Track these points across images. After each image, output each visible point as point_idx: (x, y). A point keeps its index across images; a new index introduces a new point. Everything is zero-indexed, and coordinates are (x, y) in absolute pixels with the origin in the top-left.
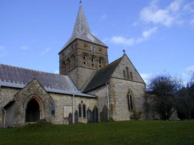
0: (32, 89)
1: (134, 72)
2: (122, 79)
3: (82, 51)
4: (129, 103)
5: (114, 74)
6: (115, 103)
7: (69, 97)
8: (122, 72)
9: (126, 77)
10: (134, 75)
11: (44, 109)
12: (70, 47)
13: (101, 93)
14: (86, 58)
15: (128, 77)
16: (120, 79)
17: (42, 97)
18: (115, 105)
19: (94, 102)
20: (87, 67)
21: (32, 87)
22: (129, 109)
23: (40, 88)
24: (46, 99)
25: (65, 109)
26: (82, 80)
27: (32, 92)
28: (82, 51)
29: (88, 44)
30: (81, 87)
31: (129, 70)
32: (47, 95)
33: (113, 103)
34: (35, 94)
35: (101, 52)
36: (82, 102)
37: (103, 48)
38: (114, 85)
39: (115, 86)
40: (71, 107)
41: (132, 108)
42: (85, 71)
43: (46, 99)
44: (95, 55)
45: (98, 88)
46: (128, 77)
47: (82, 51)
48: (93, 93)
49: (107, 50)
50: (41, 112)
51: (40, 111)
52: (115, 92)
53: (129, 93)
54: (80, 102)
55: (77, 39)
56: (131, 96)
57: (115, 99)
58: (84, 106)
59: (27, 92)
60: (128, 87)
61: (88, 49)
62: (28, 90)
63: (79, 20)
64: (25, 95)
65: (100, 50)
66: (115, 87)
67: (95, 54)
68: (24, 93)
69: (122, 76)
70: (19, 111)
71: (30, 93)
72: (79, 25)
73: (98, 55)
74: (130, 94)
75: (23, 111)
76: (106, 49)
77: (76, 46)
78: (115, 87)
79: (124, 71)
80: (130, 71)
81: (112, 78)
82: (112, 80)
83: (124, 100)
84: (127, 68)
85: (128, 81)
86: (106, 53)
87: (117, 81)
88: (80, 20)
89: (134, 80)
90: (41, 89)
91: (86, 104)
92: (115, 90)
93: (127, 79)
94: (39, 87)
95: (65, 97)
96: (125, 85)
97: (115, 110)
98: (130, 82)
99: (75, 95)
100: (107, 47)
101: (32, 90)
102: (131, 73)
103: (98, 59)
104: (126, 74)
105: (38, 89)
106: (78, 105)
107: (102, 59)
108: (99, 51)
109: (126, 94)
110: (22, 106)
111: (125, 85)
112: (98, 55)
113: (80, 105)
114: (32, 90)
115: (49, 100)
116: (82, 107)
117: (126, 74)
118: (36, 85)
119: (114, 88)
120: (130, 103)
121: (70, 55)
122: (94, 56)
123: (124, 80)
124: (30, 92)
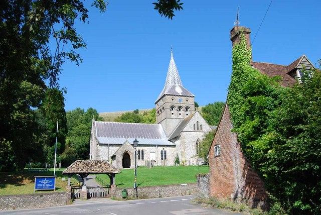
10: (203, 127)
15: (198, 129)
46: (198, 129)
58: (165, 152)
65: (187, 101)
69: (192, 129)
73: (184, 105)
80: (199, 124)
113: (162, 151)
116: (163, 153)
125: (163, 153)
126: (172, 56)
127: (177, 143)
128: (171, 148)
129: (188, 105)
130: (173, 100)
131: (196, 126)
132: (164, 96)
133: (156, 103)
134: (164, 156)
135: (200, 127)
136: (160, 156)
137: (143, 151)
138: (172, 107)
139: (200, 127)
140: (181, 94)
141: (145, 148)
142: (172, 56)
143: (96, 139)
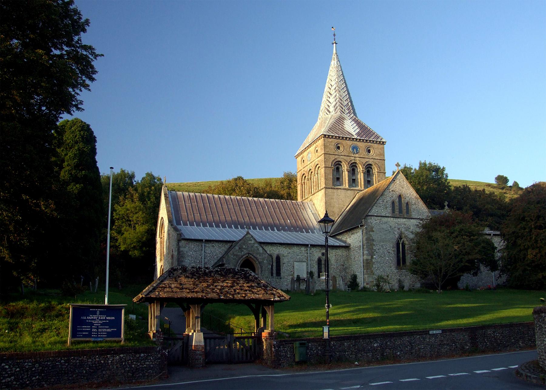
0: (244, 247)
2: (389, 217)
4: (398, 257)
5: (374, 211)
6: (372, 257)
7: (303, 249)
8: (389, 205)
9: (397, 211)
12: (312, 148)
13: (354, 239)
15: (401, 211)
16: (384, 217)
17: (258, 256)
19: (344, 254)
23: (255, 245)
24: (263, 259)
25: (296, 267)
27: (245, 251)
29: (344, 142)
34: (248, 254)
38: (372, 228)
39: (374, 229)
40: (305, 264)
43: (263, 259)
45: (351, 230)
47: (332, 158)
48: (344, 237)
49: (384, 148)
52: (373, 240)
53: (401, 238)
54: (320, 255)
58: (327, 260)
60: (399, 229)
63: (330, 87)
64: (237, 255)
66: (373, 231)
68: (235, 253)
69: (388, 211)
76: (381, 146)
78: (373, 231)
79: (393, 203)
81: (369, 217)
82: (369, 221)
83: (389, 252)
85: (399, 220)
86: (383, 154)
87: (378, 221)
89: (414, 216)
92: (374, 236)
95: (296, 249)
96: (393, 227)
97: (371, 269)
98: (404, 220)
99: (311, 245)
100: (383, 143)
102: (407, 204)
104: (397, 208)
105: (252, 247)
106: (316, 260)
109: (395, 241)
111: (393, 227)
113: (319, 261)
114: (245, 249)
117: (397, 208)
119: (371, 233)
120: (401, 256)
121: (313, 163)
123: (392, 219)
131: (397, 204)
136: (315, 270)
137: (278, 258)
139: (404, 207)
140: (356, 137)
141: (283, 251)
143: (176, 229)
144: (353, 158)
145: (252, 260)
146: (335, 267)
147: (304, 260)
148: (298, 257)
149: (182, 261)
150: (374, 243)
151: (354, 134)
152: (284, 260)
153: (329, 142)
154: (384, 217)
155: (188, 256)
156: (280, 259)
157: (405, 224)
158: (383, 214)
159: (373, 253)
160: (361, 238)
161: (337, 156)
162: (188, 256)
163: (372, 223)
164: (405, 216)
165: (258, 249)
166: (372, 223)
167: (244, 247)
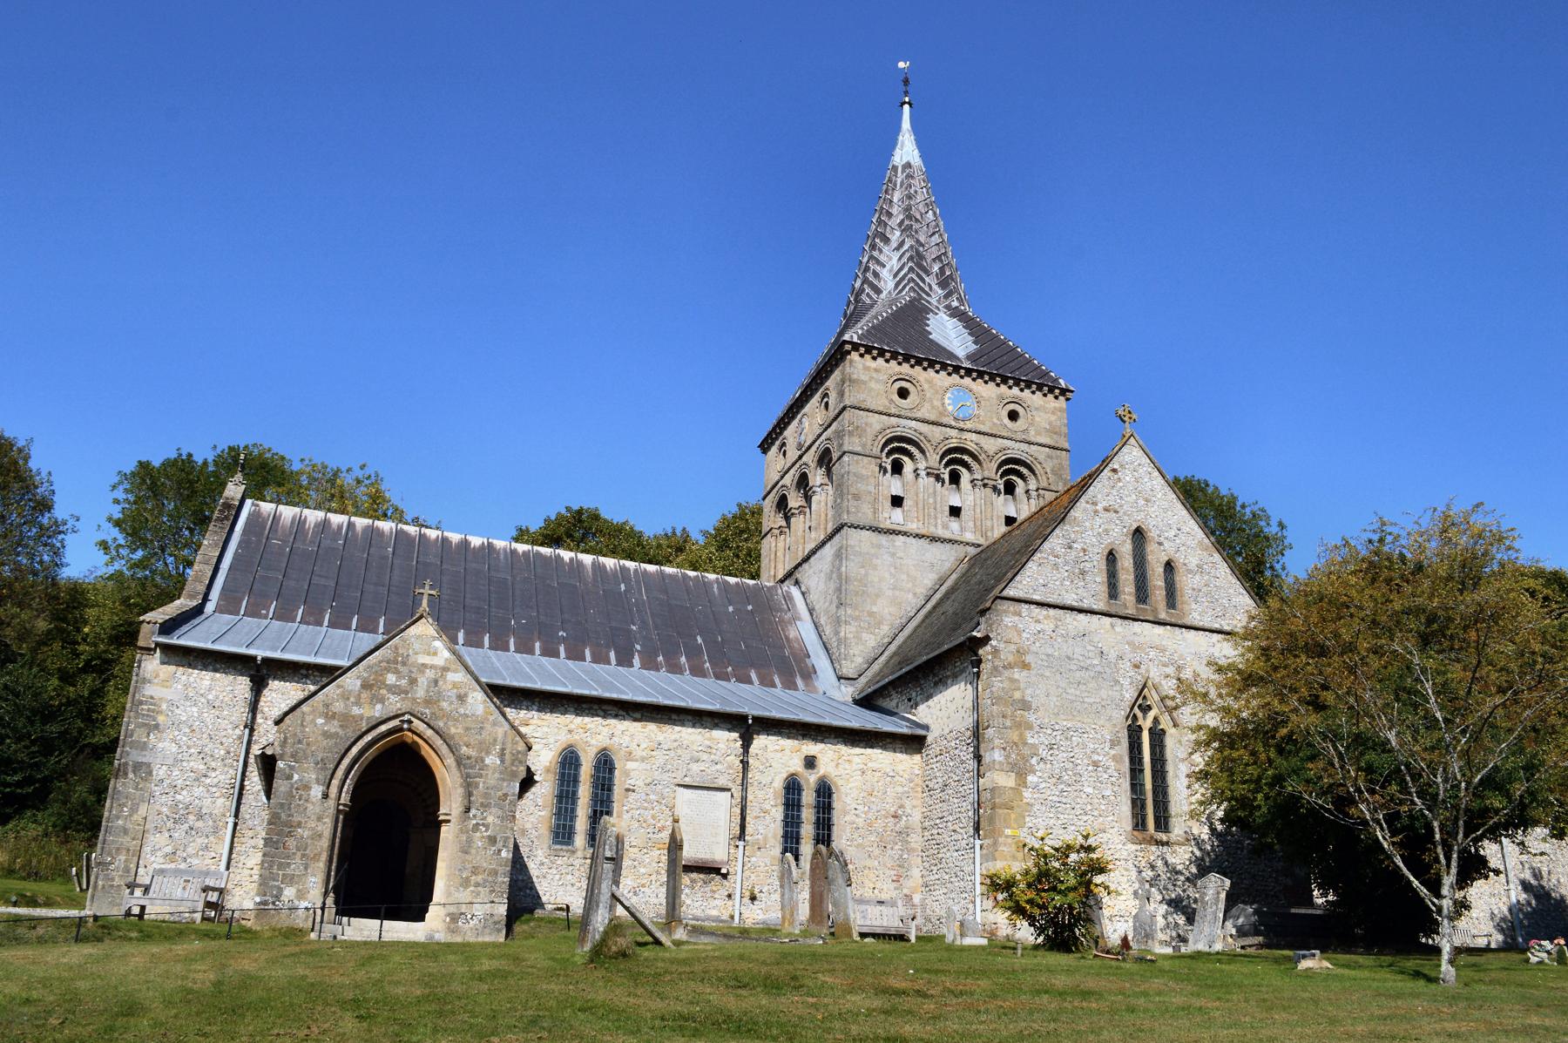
1: (1193, 562)
3: (876, 422)
4: (1136, 786)
10: (1187, 583)
11: (468, 810)
14: (908, 466)
15: (1142, 594)
16: (1072, 609)
18: (1016, 791)
19: (899, 768)
20: (913, 527)
21: (397, 672)
22: (1139, 823)
23: (451, 676)
26: (871, 614)
27: (395, 703)
28: (878, 427)
30: (859, 660)
31: (1151, 548)
32: (494, 724)
33: (1006, 780)
35: (1020, 424)
36: (810, 762)
37: (1034, 399)
39: (1028, 659)
41: (1163, 822)
42: (893, 555)
44: (971, 447)
46: (1142, 594)
50: (444, 829)
51: (437, 825)
52: (1025, 706)
53: (1146, 709)
54: (797, 765)
55: (848, 347)
56: (1158, 736)
57: (1026, 751)
58: (825, 792)
59: (358, 703)
60: (1137, 666)
61: (924, 413)
62: (366, 686)
64: (346, 719)
65: (1013, 416)
66: (1026, 666)
67: (971, 441)
68: (338, 707)
69: (1093, 592)
70: (297, 818)
71: (379, 706)
72: (882, 258)
73: (990, 445)
74: (1151, 714)
75: (319, 819)
77: (841, 394)
78: (1026, 666)
79: (1111, 557)
82: (1008, 620)
83: (1096, 764)
84: (1139, 534)
85: (1137, 626)
87: (1048, 626)
88: (894, 222)
89: (1194, 618)
90: (455, 685)
91: (840, 783)
93: (1131, 611)
94: (445, 669)
96: (1112, 655)
101: (393, 690)
102: (1169, 566)
103: (990, 470)
106: (779, 784)
107: (1024, 471)
108: (1006, 421)
109: (1119, 716)
110: (317, 791)
111: (1112, 655)
112: (990, 445)
113: (792, 788)
114: (393, 690)
115: (502, 755)
116: (808, 798)
118: (426, 660)
119: (1016, 674)
120: (1149, 786)
121: (814, 448)
122: (966, 458)
123: (1108, 620)
124: (382, 700)
125: (808, 798)
126: (906, 124)
127: (946, 710)
128: (879, 757)
129: (1017, 450)
130: (903, 393)
131: (1126, 562)
132: (844, 408)
133: (765, 446)
134: (807, 830)
135: (1157, 580)
137: (605, 765)
138: (898, 450)
139: (1157, 580)
142: (906, 124)
144: (954, 433)
145: (426, 751)
146: (860, 822)
147: (722, 782)
148: (695, 767)
149: (143, 747)
150: (1032, 717)
151: (961, 352)
152: (629, 774)
153: (867, 368)
154: (1072, 609)
155: (176, 725)
156: (611, 770)
157: (1163, 650)
158: (1070, 600)
159: (1025, 759)
160: (947, 565)
161: (894, 420)
162: (176, 725)
163: (1019, 632)
164: (1163, 616)
165: (462, 698)
166: (1019, 632)
167: (391, 679)
